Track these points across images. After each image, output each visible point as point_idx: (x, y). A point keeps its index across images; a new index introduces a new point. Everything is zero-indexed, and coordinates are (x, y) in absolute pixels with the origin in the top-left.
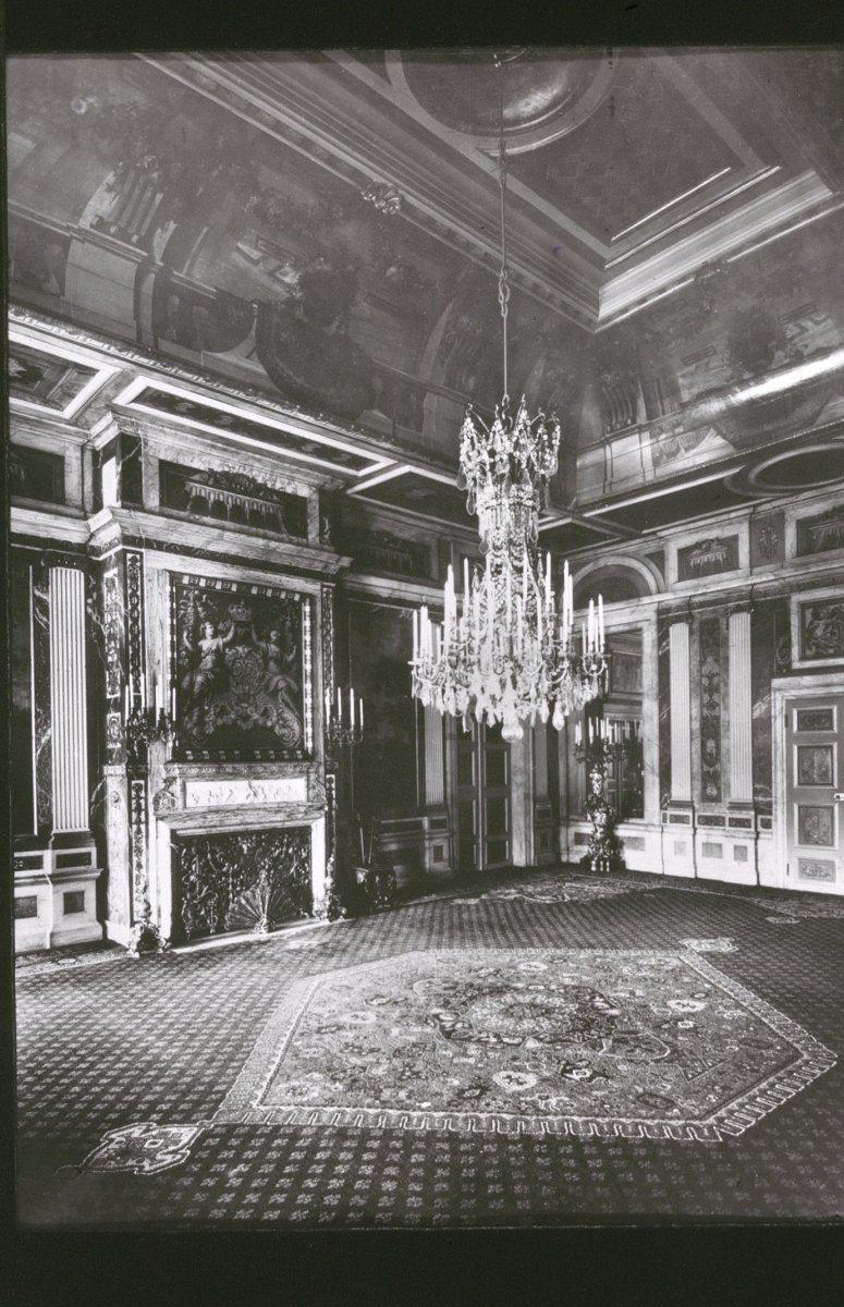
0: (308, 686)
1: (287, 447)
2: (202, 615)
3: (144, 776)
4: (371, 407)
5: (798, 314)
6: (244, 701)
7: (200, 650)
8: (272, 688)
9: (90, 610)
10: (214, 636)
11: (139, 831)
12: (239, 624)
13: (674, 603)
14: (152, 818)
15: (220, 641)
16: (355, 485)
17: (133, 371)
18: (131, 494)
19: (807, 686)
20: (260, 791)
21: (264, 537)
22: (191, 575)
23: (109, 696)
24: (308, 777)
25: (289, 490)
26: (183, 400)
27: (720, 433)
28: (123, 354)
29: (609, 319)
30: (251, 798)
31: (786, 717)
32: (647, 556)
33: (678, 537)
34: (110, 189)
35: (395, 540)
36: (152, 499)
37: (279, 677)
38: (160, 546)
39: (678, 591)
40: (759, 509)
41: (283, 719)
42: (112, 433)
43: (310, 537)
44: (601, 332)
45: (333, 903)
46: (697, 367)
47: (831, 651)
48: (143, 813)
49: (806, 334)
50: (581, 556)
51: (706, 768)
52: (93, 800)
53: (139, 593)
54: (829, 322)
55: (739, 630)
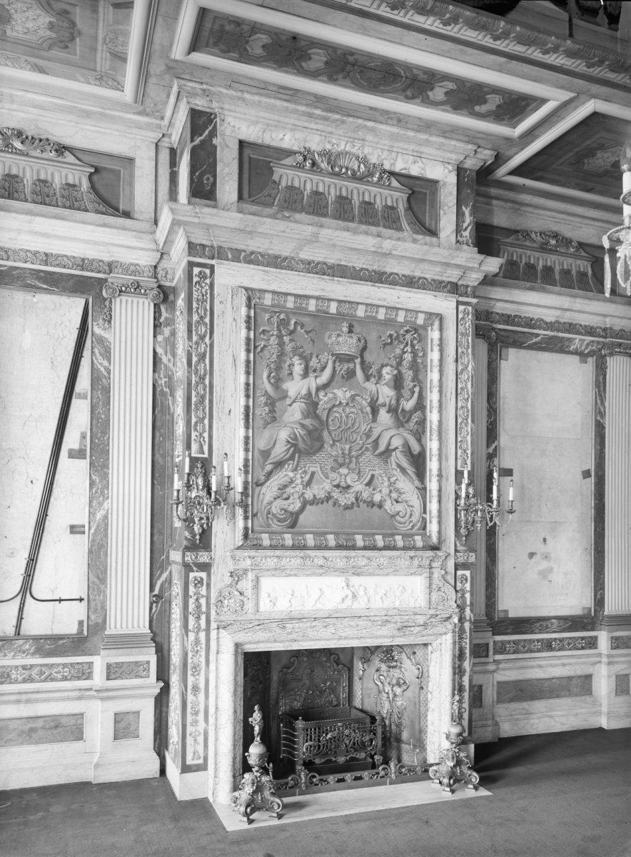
3: (205, 567)
6: (341, 465)
7: (284, 396)
11: (197, 642)
12: (341, 358)
14: (213, 625)
16: (510, 158)
20: (362, 593)
22: (274, 292)
24: (431, 573)
25: (415, 171)
30: (348, 602)
35: (568, 242)
36: (228, 187)
37: (393, 432)
38: (238, 256)
41: (398, 490)
43: (443, 235)
45: (459, 763)
48: (203, 617)
53: (207, 320)
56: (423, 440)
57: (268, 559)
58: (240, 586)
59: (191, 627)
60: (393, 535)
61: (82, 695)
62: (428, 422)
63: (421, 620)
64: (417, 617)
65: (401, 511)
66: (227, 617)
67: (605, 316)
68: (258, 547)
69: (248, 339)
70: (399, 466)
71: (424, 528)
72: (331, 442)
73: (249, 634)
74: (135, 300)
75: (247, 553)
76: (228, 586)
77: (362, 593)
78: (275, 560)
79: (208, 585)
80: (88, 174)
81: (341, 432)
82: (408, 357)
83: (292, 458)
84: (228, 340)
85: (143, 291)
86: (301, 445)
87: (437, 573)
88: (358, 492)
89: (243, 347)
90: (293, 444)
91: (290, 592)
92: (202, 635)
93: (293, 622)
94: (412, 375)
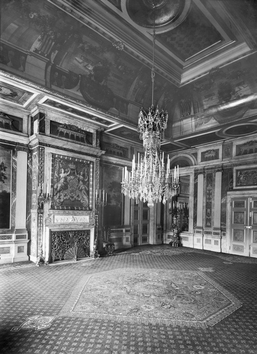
0: (91, 189)
1: (87, 118)
2: (61, 167)
3: (42, 213)
4: (113, 107)
5: (239, 85)
7: (60, 177)
8: (80, 189)
9: (28, 164)
10: (64, 173)
11: (40, 229)
12: (72, 169)
13: (199, 168)
14: (44, 225)
15: (66, 174)
16: (107, 130)
17: (44, 94)
18: (42, 130)
19: (237, 194)
20: (76, 219)
21: (80, 144)
22: (58, 154)
23: (33, 189)
25: (88, 130)
26: (58, 103)
27: (215, 119)
28: (41, 89)
29: (183, 83)
30: (73, 221)
31: (231, 203)
32: (192, 154)
33: (201, 149)
34: (39, 40)
35: (118, 146)
36: (48, 132)
37: (83, 186)
38: (50, 146)
39: (201, 165)
40: (226, 141)
41: (83, 198)
42: (37, 112)
43: (93, 145)
44: (181, 87)
45: (96, 253)
46: (209, 99)
47: (245, 184)
48: (42, 224)
49: (241, 90)
50: (173, 153)
51: (207, 217)
52: (27, 219)
53: (43, 159)
54: (248, 87)
55: (218, 177)
59: (39, 226)
60: (82, 207)
61: (10, 242)
66: (47, 224)
67: (126, 163)
68: (54, 209)
69: (52, 164)
70: (84, 193)
71: (89, 206)
75: (52, 210)
79: (43, 217)
82: (86, 170)
86: (63, 188)
89: (51, 166)
90: (61, 187)
92: (41, 228)
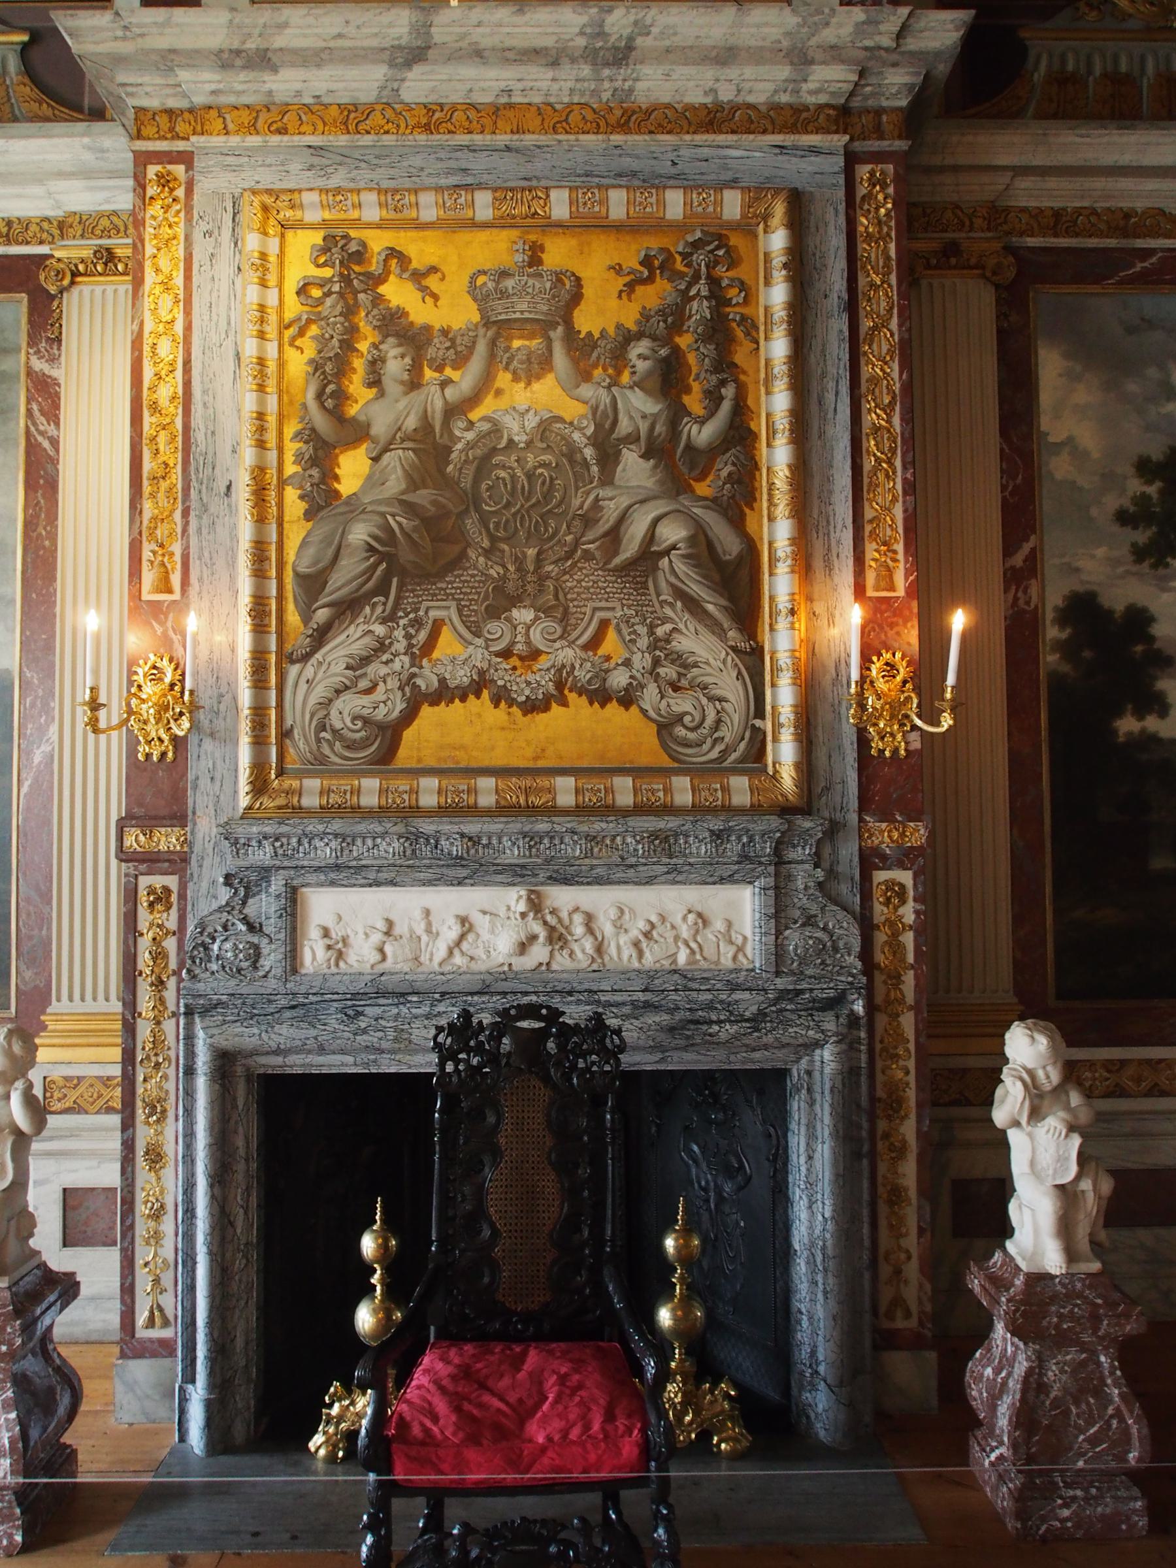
30: (539, 953)
41: (678, 659)
56: (750, 516)
57: (317, 843)
58: (251, 910)
62: (764, 471)
63: (749, 1003)
64: (738, 995)
65: (687, 713)
70: (680, 594)
72: (486, 544)
73: (256, 1031)
74: (110, 289)
76: (220, 909)
77: (579, 930)
78: (333, 844)
80: (19, 48)
81: (515, 515)
83: (382, 589)
84: (223, 325)
85: (120, 267)
86: (406, 555)
87: (803, 877)
88: (564, 666)
91: (381, 925)
93: (382, 1001)
94: (713, 354)
